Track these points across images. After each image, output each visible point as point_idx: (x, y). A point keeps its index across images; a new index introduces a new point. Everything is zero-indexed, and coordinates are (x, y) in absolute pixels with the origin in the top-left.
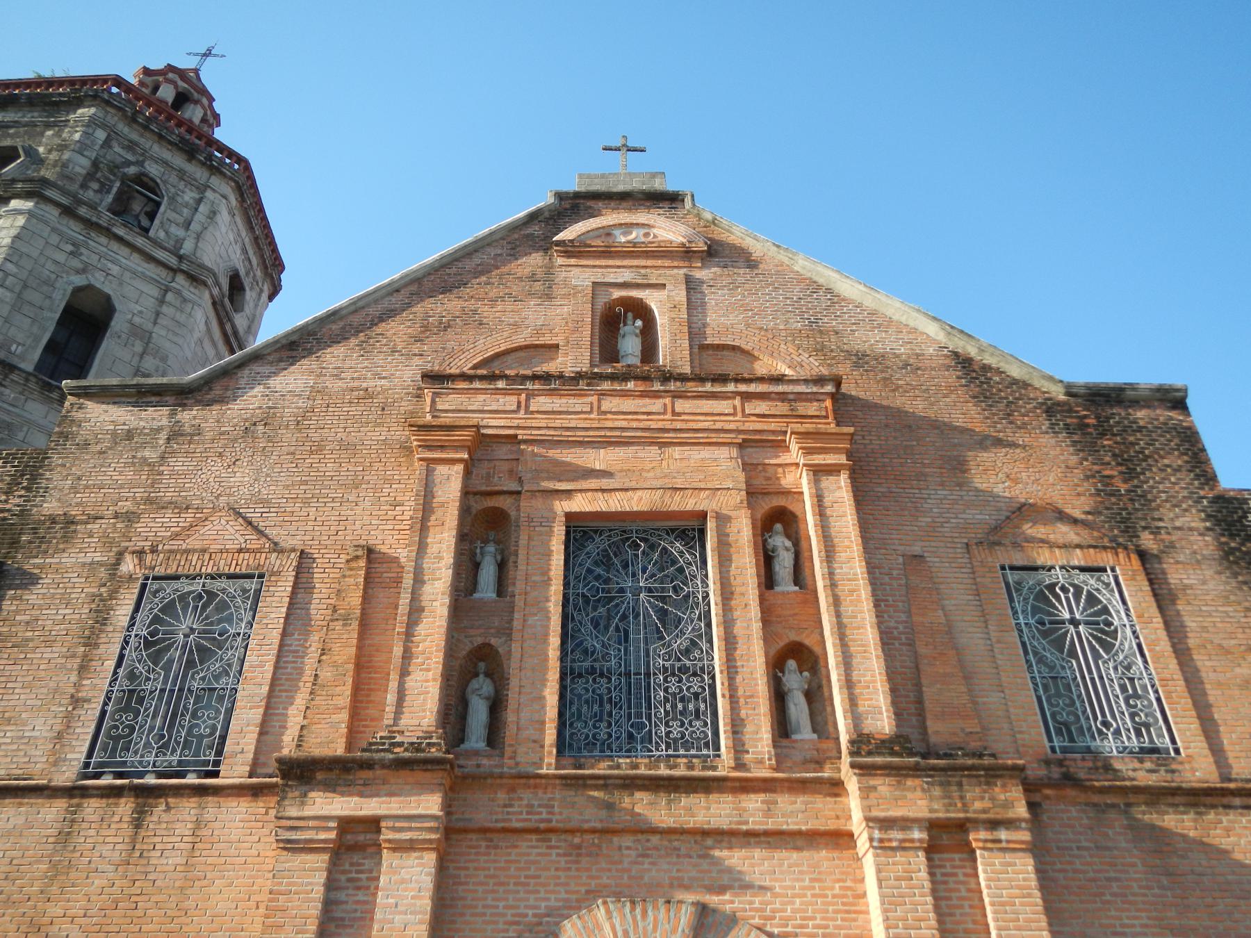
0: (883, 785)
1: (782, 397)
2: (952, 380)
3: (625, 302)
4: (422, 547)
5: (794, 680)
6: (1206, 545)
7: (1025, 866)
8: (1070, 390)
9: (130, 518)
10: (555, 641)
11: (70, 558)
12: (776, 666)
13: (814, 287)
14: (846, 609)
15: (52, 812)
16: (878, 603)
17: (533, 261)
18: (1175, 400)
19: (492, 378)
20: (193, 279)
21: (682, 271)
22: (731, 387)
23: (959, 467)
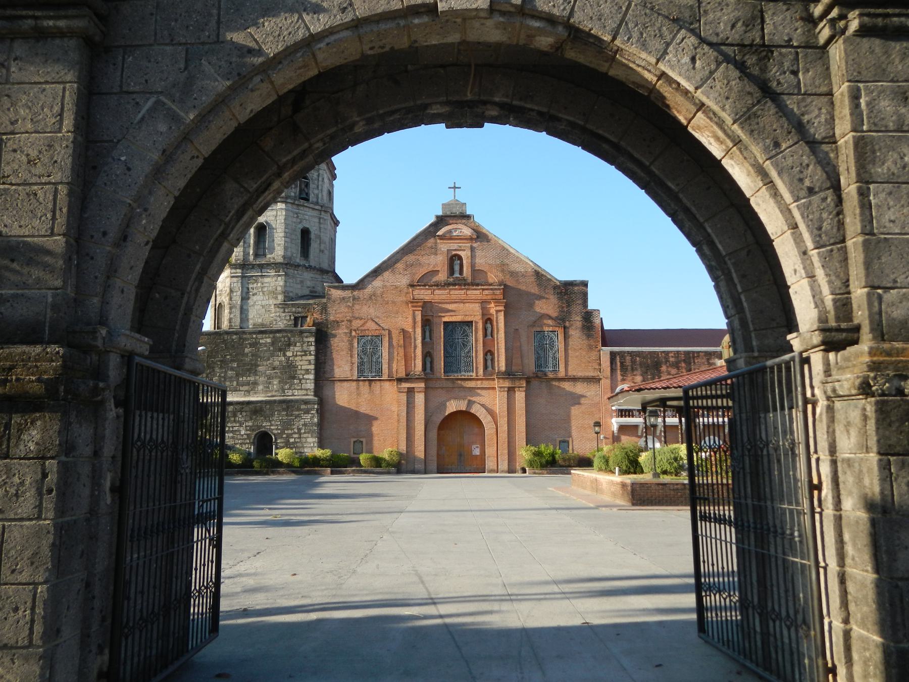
0: (501, 381)
1: (491, 289)
2: (533, 280)
3: (456, 255)
4: (415, 332)
5: (489, 357)
6: (579, 324)
7: (523, 394)
8: (560, 282)
9: (350, 321)
10: (442, 352)
11: (340, 331)
12: (485, 354)
13: (503, 249)
14: (500, 345)
15: (354, 384)
16: (506, 342)
17: (432, 240)
18: (585, 284)
19: (425, 285)
20: (325, 211)
21: (469, 245)
22: (480, 287)
23: (531, 305)
